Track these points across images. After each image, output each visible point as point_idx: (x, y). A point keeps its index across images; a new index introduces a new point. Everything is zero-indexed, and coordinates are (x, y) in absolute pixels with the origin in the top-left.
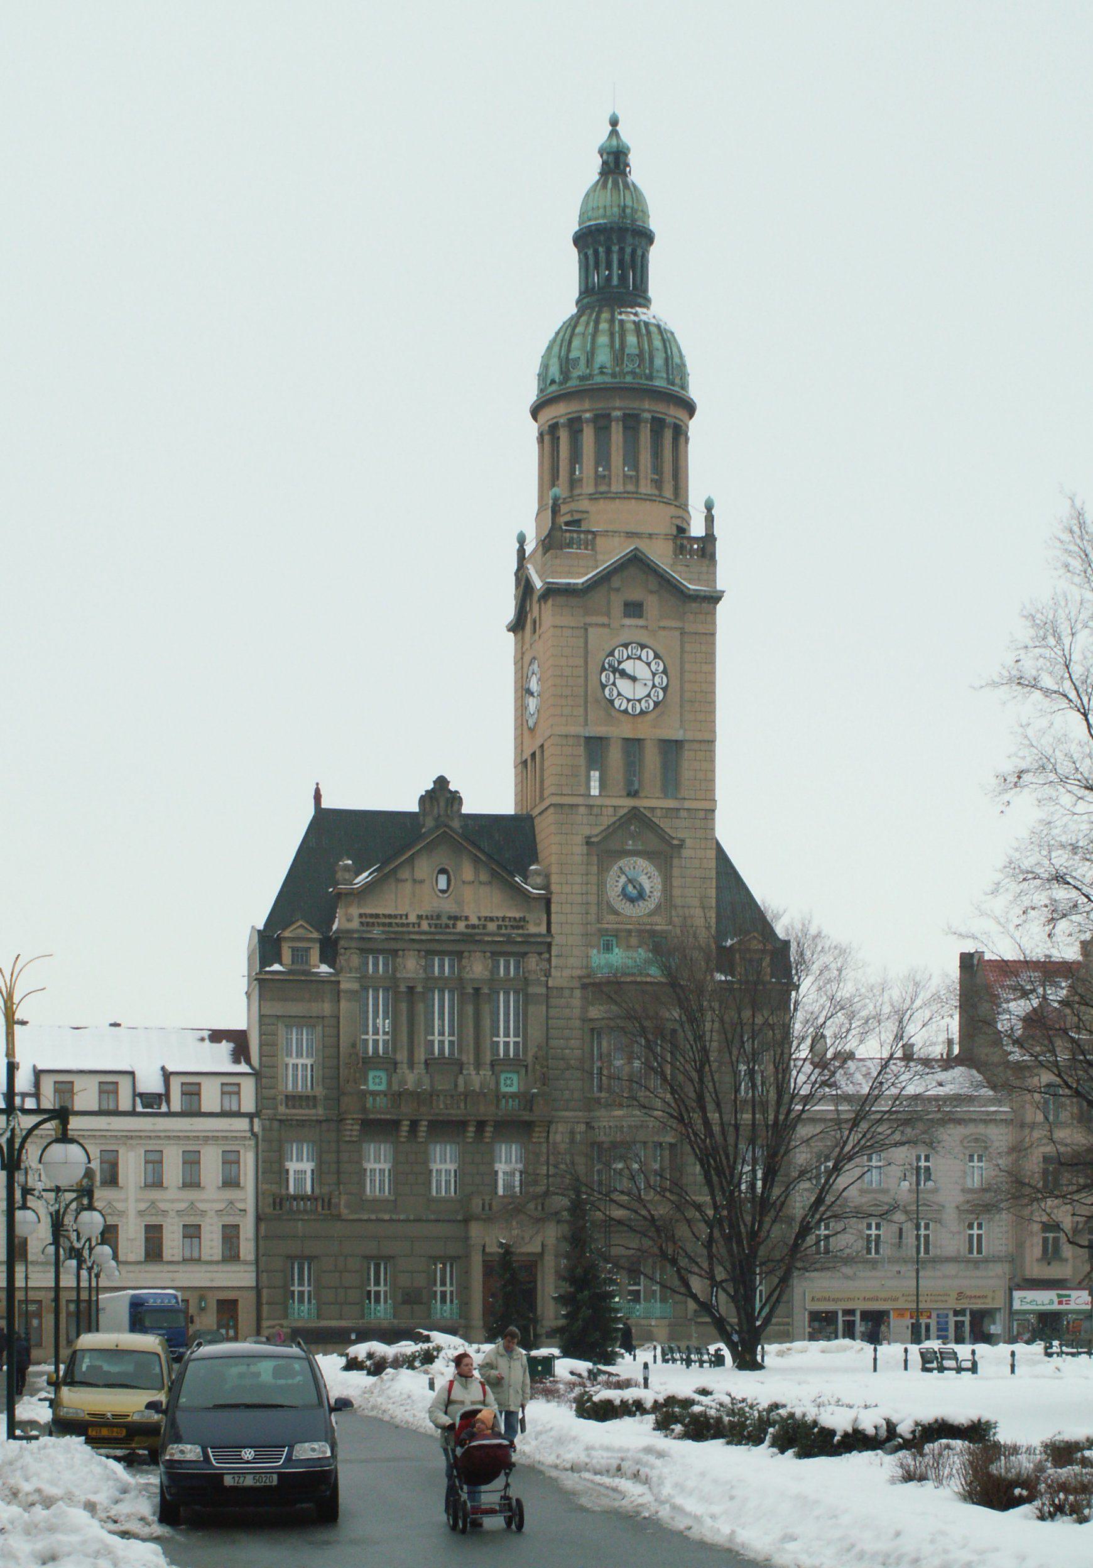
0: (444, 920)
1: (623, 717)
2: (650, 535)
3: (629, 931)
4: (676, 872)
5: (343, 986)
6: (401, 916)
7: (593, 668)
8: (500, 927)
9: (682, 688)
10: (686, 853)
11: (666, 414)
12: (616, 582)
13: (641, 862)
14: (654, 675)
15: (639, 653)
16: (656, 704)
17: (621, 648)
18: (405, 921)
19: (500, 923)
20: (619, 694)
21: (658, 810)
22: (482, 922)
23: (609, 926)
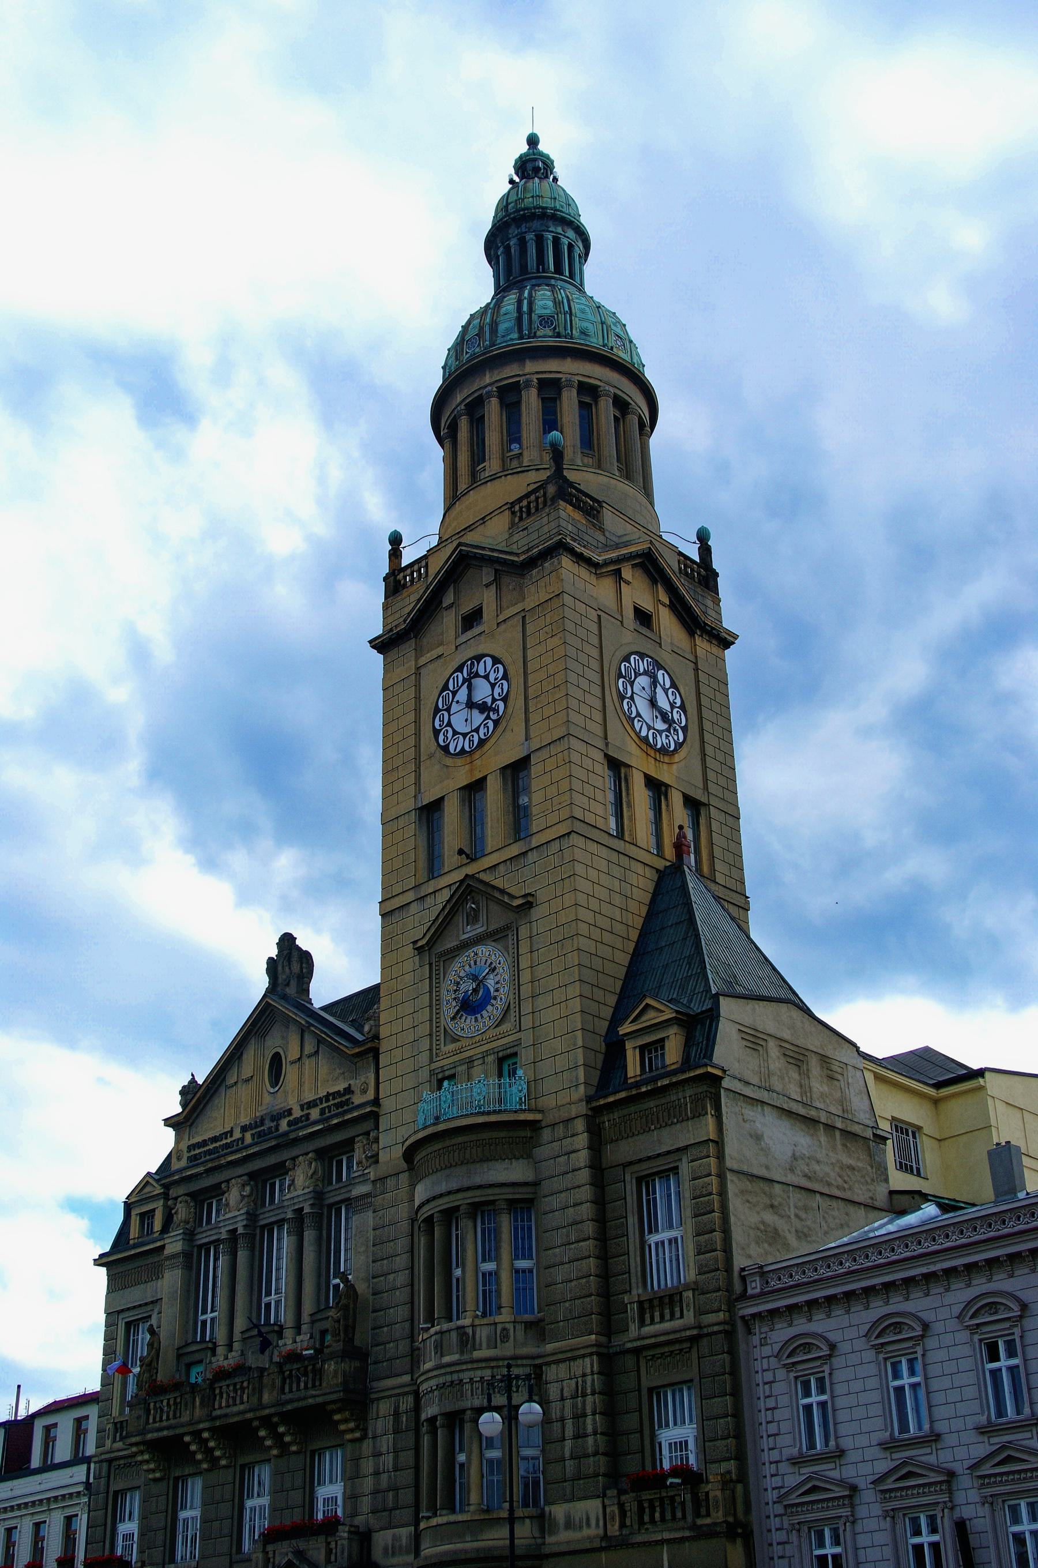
0: (268, 1124)
1: (459, 761)
2: (483, 518)
3: (470, 1062)
4: (524, 948)
5: (169, 1250)
6: (226, 1133)
7: (426, 713)
9: (526, 688)
10: (536, 913)
11: (519, 375)
12: (448, 599)
13: (483, 951)
14: (493, 686)
15: (474, 670)
16: (496, 723)
17: (455, 675)
18: (229, 1141)
19: (325, 1105)
20: (455, 733)
21: (502, 868)
22: (306, 1112)
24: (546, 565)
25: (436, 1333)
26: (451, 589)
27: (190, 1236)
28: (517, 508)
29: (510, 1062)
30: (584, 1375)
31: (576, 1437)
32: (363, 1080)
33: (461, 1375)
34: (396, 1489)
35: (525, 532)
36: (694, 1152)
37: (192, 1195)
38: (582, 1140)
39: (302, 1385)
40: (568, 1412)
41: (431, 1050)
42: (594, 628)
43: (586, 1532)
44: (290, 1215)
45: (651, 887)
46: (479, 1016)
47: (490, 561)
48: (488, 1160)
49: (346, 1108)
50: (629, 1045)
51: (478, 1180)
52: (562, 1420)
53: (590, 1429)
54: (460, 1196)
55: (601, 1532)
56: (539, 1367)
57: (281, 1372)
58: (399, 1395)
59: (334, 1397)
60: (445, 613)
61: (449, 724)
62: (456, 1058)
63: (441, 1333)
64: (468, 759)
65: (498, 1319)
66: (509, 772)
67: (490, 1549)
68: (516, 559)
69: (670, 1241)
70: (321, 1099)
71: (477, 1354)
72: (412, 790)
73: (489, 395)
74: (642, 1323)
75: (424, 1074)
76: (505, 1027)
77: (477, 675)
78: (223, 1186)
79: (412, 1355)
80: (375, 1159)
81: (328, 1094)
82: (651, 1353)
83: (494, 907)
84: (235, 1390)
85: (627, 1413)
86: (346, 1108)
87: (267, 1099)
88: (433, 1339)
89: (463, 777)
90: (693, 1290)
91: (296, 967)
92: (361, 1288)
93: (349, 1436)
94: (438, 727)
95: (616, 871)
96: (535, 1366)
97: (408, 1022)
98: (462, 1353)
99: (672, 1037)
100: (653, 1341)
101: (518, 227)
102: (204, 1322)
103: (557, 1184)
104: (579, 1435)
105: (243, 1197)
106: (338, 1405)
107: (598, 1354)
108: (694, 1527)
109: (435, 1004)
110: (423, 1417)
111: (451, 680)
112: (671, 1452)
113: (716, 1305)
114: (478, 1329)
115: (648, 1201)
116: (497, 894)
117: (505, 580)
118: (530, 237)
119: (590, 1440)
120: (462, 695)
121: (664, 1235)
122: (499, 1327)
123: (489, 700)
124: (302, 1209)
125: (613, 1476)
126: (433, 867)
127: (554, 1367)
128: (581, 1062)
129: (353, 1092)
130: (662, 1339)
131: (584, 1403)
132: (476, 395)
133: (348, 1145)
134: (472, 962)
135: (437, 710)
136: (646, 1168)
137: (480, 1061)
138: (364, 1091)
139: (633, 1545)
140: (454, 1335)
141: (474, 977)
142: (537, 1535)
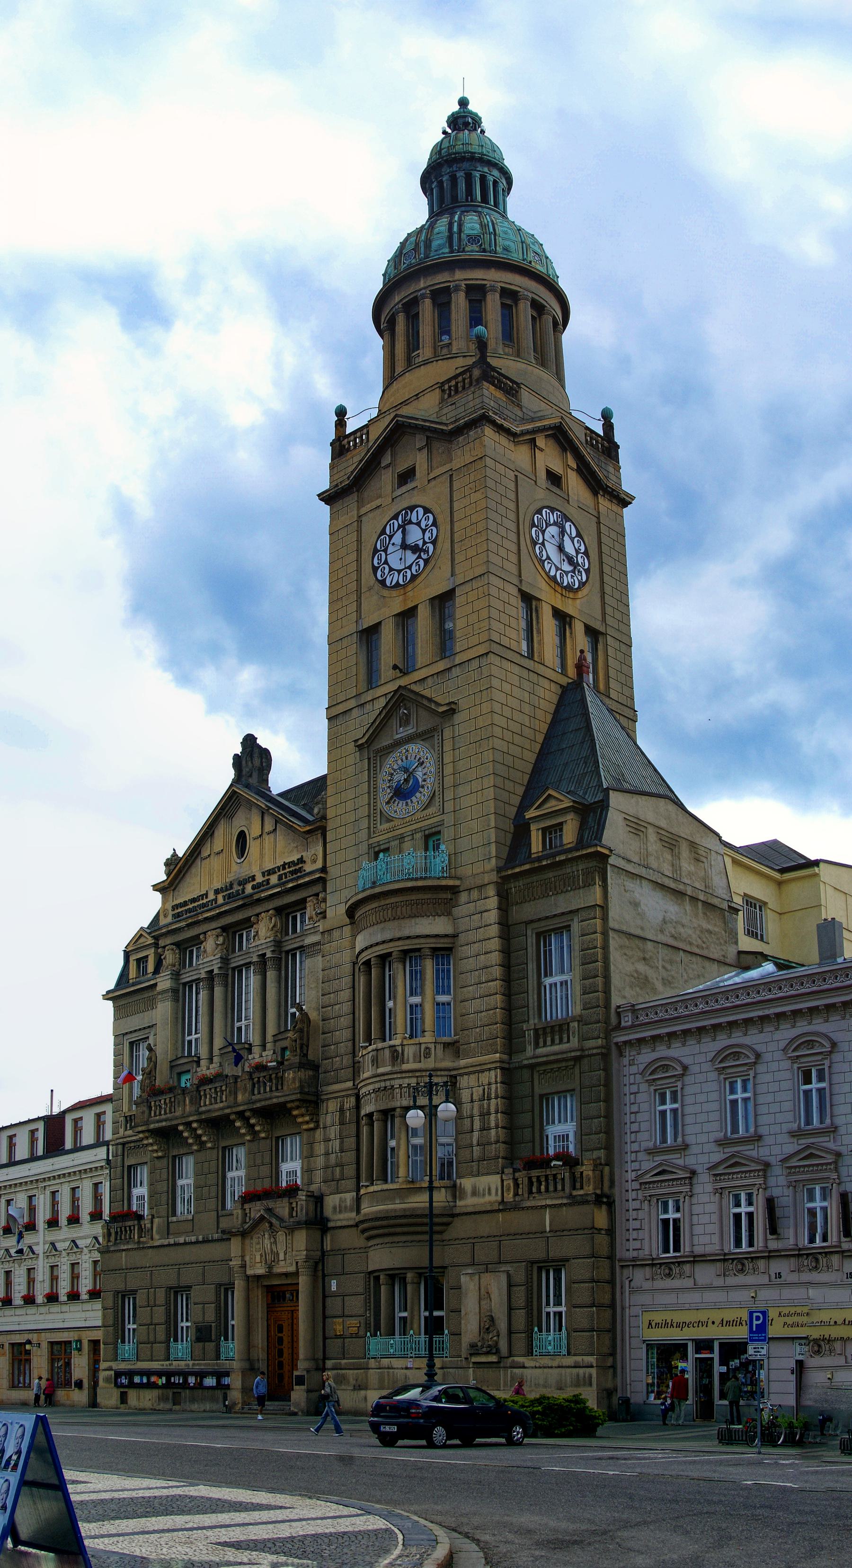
0: (236, 887)
1: (394, 593)
3: (402, 838)
4: (448, 746)
6: (202, 896)
8: (280, 878)
10: (458, 718)
12: (386, 460)
13: (415, 749)
14: (424, 531)
15: (408, 518)
16: (426, 562)
18: (205, 901)
19: (282, 872)
20: (391, 569)
21: (430, 680)
22: (267, 878)
23: (381, 838)
24: (471, 433)
25: (373, 1051)
26: (389, 452)
27: (176, 975)
28: (446, 387)
29: (435, 838)
30: (490, 1084)
31: (483, 1129)
32: (313, 852)
33: (393, 1082)
34: (341, 1165)
35: (453, 406)
36: (584, 914)
37: (177, 944)
38: (493, 902)
39: (268, 1089)
40: (476, 1112)
41: (369, 828)
42: (512, 486)
43: (487, 1198)
44: (255, 959)
45: (555, 699)
46: (409, 801)
47: (423, 429)
48: (415, 916)
49: (299, 874)
50: (533, 827)
51: (406, 932)
52: (472, 1117)
53: (493, 1124)
54: (391, 944)
55: (499, 1198)
56: (455, 1077)
57: (251, 1079)
58: (343, 1096)
59: (293, 1097)
60: (383, 472)
61: (386, 562)
62: (390, 835)
63: (377, 1050)
64: (402, 591)
65: (422, 1040)
66: (437, 602)
67: (414, 1209)
68: (445, 428)
69: (561, 983)
70: (278, 868)
71: (405, 1067)
72: (354, 616)
73: (423, 296)
74: (537, 1045)
75: (364, 848)
76: (430, 810)
77: (410, 522)
78: (201, 937)
79: (354, 1067)
80: (323, 915)
81: (285, 864)
82: (543, 1068)
83: (423, 713)
84: (216, 1092)
85: (523, 1113)
86: (299, 874)
87: (235, 867)
88: (370, 1055)
89: (397, 605)
90: (578, 1021)
91: (257, 762)
92: (313, 1015)
93: (305, 1127)
94: (376, 564)
95: (526, 685)
96: (451, 1076)
97: (350, 806)
98: (393, 1065)
99: (569, 822)
100: (544, 1059)
101: (450, 167)
102: (190, 1042)
103: (471, 936)
104: (484, 1128)
105: (217, 945)
106: (297, 1103)
107: (502, 1069)
108: (571, 1196)
109: (372, 791)
110: (363, 1113)
111: (388, 526)
112: (555, 1142)
113: (596, 1034)
114: (406, 1048)
115: (545, 952)
116: (425, 702)
117: (436, 445)
118: (460, 174)
119: (493, 1132)
120: (398, 538)
121: (557, 979)
122: (423, 1046)
123: (420, 543)
124: (265, 954)
125: (510, 1159)
126: (372, 679)
127: (466, 1077)
128: (493, 839)
129: (305, 862)
130: (552, 1058)
131: (489, 1105)
132: (412, 296)
133: (301, 904)
134: (404, 758)
135: (376, 551)
136: (543, 926)
137: (410, 838)
138: (314, 861)
139: (523, 1208)
140: (387, 1052)
141: (406, 770)
142: (449, 1199)
